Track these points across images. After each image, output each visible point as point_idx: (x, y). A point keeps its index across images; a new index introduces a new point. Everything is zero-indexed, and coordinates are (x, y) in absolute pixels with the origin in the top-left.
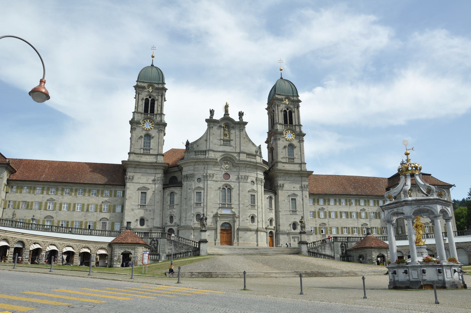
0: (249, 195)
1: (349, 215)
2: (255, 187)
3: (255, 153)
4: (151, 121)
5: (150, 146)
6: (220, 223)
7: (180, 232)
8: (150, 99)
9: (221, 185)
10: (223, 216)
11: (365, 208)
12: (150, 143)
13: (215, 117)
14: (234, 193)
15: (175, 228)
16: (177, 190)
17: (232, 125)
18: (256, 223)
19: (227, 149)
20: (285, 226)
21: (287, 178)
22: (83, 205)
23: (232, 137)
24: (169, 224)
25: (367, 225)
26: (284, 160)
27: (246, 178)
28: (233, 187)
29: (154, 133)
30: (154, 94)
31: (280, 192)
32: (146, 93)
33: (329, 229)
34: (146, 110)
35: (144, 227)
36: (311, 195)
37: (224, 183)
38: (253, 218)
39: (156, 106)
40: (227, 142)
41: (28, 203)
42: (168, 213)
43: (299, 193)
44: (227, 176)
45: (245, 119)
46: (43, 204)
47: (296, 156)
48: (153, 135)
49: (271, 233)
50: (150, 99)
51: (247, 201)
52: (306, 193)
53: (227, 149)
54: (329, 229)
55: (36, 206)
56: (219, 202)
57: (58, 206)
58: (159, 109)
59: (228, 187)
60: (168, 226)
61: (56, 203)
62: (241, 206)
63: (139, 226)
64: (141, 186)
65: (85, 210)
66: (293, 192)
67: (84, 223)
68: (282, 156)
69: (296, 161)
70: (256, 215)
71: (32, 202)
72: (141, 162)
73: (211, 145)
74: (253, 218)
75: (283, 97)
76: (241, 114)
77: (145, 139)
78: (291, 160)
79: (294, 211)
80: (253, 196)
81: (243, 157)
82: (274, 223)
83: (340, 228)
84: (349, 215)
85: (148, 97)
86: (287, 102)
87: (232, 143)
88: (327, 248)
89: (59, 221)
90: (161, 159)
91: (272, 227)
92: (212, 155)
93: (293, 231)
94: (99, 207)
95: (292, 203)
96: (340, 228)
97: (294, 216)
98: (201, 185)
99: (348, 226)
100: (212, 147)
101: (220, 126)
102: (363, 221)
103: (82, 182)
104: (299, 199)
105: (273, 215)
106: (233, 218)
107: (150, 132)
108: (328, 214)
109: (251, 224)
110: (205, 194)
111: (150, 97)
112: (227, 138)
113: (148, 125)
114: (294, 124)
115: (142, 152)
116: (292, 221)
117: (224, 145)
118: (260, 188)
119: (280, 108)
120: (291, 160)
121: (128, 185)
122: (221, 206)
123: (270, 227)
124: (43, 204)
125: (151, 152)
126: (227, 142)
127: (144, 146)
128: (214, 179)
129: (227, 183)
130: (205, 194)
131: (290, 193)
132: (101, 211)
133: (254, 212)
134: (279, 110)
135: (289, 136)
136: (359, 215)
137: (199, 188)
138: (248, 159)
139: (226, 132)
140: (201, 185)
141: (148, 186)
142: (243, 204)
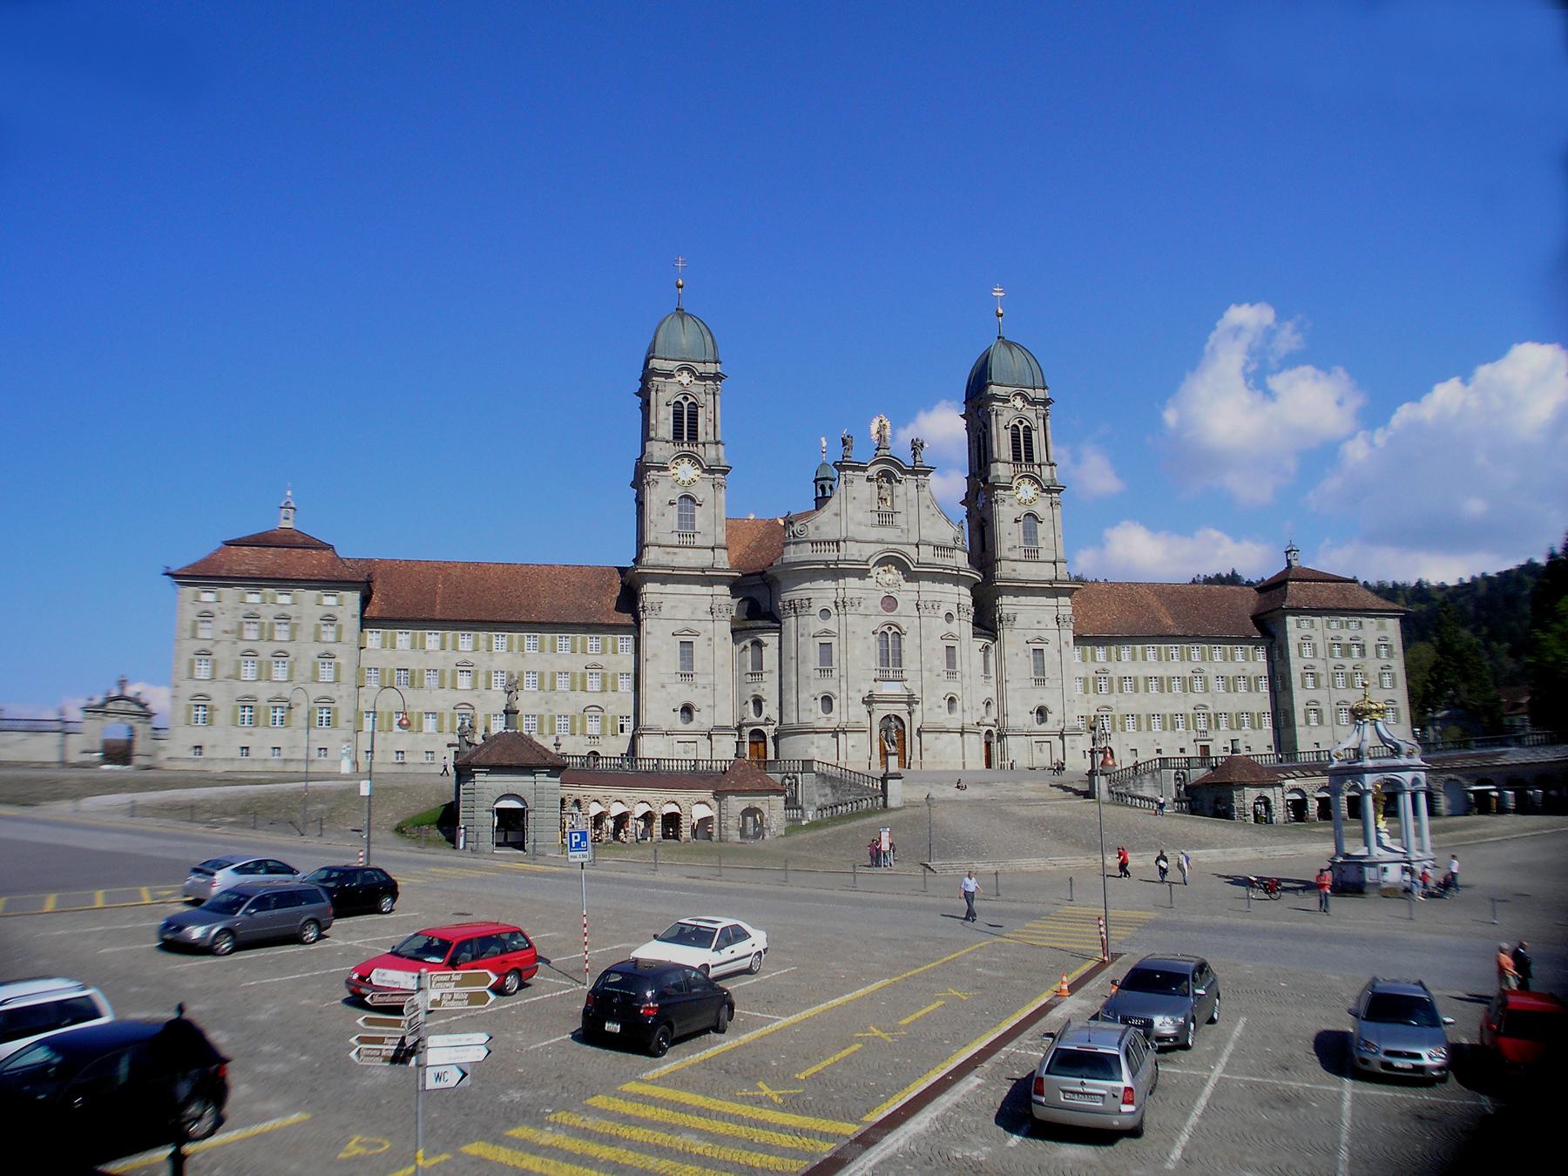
1: (1163, 684)
2: (954, 627)
3: (952, 544)
4: (694, 459)
5: (693, 527)
6: (878, 715)
7: (782, 742)
8: (686, 404)
9: (877, 622)
11: (1203, 666)
12: (693, 518)
13: (856, 456)
14: (908, 644)
15: (769, 731)
16: (770, 640)
17: (899, 475)
18: (957, 714)
20: (1019, 717)
21: (1022, 599)
22: (542, 675)
23: (899, 505)
24: (751, 716)
25: (1205, 707)
26: (1015, 555)
27: (936, 605)
28: (904, 629)
29: (703, 490)
30: (694, 389)
31: (1006, 634)
32: (677, 388)
33: (1118, 718)
34: (678, 435)
35: (692, 726)
36: (1080, 640)
37: (884, 619)
39: (700, 420)
40: (886, 519)
41: (413, 672)
42: (749, 693)
43: (1051, 635)
44: (890, 603)
45: (926, 458)
46: (448, 675)
47: (1041, 544)
48: (700, 498)
49: (989, 733)
50: (686, 404)
51: (940, 663)
52: (1070, 636)
53: (888, 534)
54: (1118, 718)
55: (431, 681)
56: (873, 666)
57: (482, 678)
58: (711, 430)
59: (895, 629)
60: (751, 725)
61: (476, 672)
62: (925, 674)
63: (680, 726)
64: (679, 626)
65: (547, 687)
66: (1036, 633)
67: (546, 719)
69: (1043, 555)
71: (421, 672)
72: (679, 568)
73: (851, 527)
75: (1010, 390)
76: (916, 446)
77: (680, 509)
78: (1032, 555)
79: (1040, 682)
81: (927, 554)
82: (993, 709)
83: (1143, 717)
84: (1163, 684)
85: (680, 398)
86: (1019, 403)
87: (899, 519)
88: (1146, 783)
89: (488, 716)
90: (723, 560)
92: (852, 551)
93: (1037, 727)
94: (578, 680)
95: (1035, 660)
96: (1143, 717)
97: (1039, 692)
98: (831, 624)
99: (1161, 712)
100: (855, 531)
101: (869, 479)
102: (1196, 698)
103: (534, 618)
104: (1050, 651)
105: (991, 692)
106: (909, 704)
107: (693, 491)
108: (1116, 685)
110: (843, 647)
111: (686, 399)
112: (885, 507)
113: (686, 471)
114: (1037, 460)
115: (675, 540)
116: (1036, 703)
117: (881, 524)
118: (964, 627)
119: (1003, 420)
120: (1032, 555)
121: (647, 625)
122: (877, 675)
123: (987, 721)
124: (448, 675)
125: (699, 541)
126: (886, 519)
127: (680, 526)
128: (861, 610)
129: (892, 619)
130: (843, 647)
131: (1030, 636)
132: (584, 689)
133: (953, 688)
134: (1001, 427)
135: (1027, 490)
136: (1187, 685)
137: (827, 632)
138: (939, 561)
139: (884, 493)
140: (831, 624)
141: (695, 626)
142: (930, 670)
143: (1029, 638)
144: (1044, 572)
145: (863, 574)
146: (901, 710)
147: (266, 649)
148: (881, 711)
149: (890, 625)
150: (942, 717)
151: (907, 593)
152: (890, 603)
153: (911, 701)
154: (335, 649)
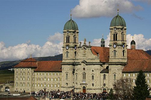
0: (91, 76)
6: (82, 86)
10: (83, 84)
19: (85, 58)
38: (93, 85)
44: (84, 69)
51: (91, 78)
53: (85, 58)
68: (111, 56)
70: (94, 83)
74: (93, 85)
80: (93, 76)
91: (106, 87)
109: (92, 86)
115: (66, 58)
125: (69, 58)
128: (80, 70)
142: (89, 80)
143: (113, 73)
144: (117, 61)
145: (80, 65)
146: (85, 86)
147: (22, 76)
148: (83, 86)
149: (84, 72)
150: (91, 87)
151: (86, 67)
152: (84, 69)
153: (86, 84)
154: (29, 76)
